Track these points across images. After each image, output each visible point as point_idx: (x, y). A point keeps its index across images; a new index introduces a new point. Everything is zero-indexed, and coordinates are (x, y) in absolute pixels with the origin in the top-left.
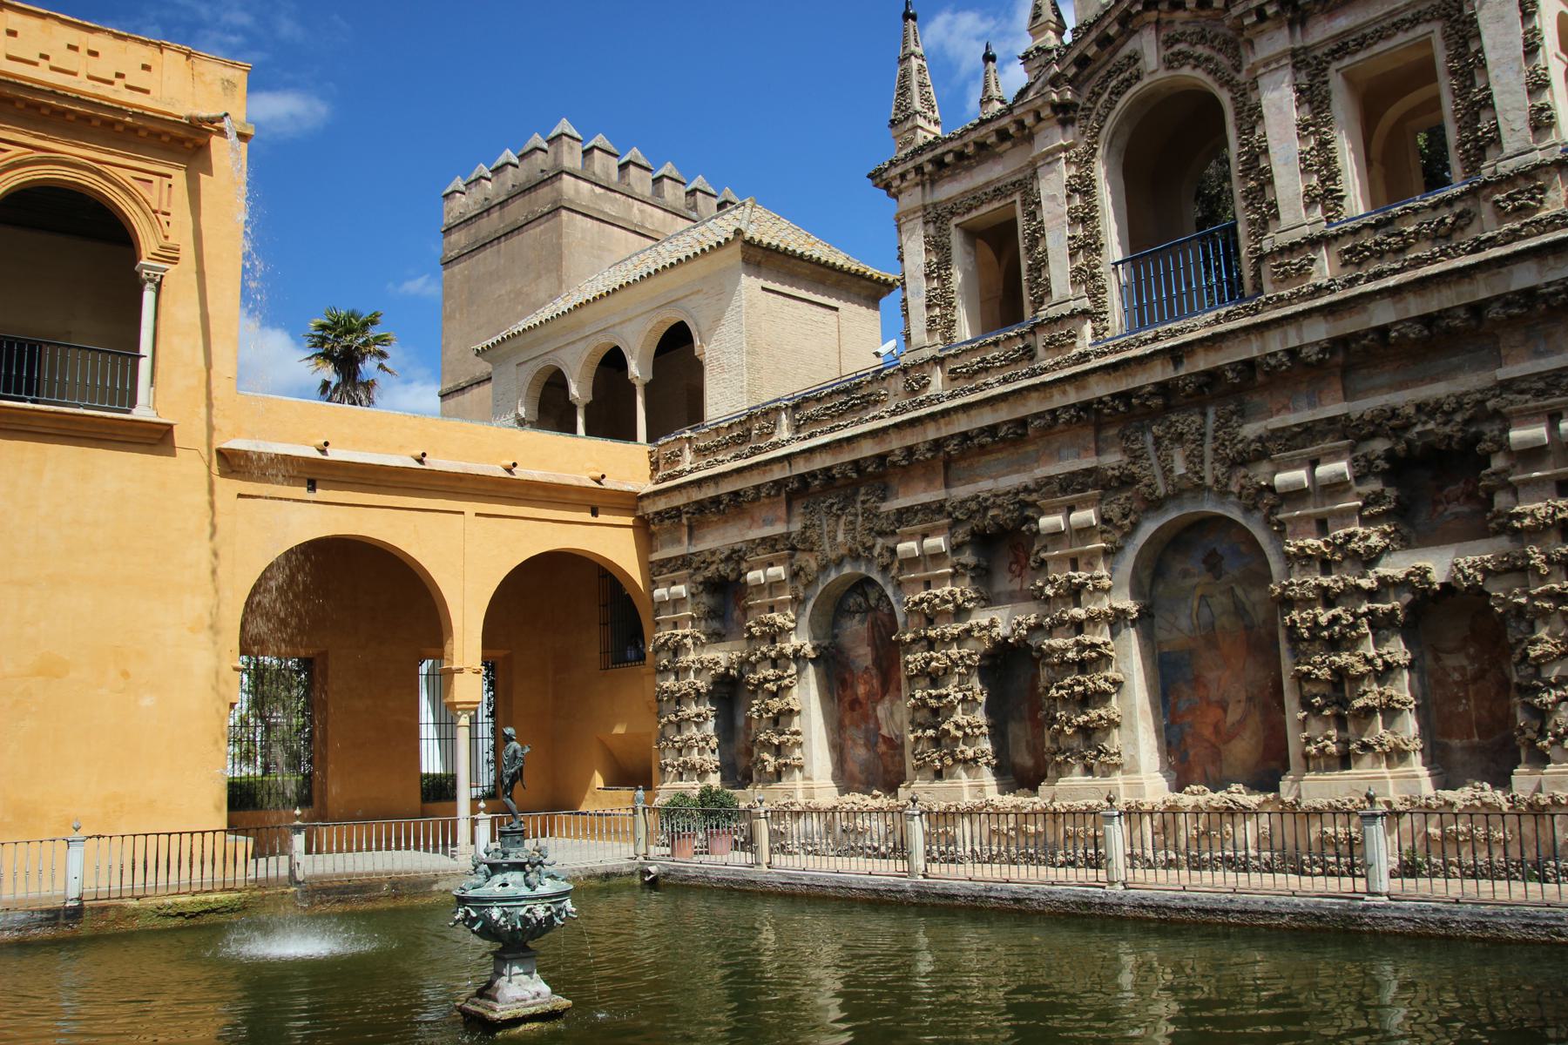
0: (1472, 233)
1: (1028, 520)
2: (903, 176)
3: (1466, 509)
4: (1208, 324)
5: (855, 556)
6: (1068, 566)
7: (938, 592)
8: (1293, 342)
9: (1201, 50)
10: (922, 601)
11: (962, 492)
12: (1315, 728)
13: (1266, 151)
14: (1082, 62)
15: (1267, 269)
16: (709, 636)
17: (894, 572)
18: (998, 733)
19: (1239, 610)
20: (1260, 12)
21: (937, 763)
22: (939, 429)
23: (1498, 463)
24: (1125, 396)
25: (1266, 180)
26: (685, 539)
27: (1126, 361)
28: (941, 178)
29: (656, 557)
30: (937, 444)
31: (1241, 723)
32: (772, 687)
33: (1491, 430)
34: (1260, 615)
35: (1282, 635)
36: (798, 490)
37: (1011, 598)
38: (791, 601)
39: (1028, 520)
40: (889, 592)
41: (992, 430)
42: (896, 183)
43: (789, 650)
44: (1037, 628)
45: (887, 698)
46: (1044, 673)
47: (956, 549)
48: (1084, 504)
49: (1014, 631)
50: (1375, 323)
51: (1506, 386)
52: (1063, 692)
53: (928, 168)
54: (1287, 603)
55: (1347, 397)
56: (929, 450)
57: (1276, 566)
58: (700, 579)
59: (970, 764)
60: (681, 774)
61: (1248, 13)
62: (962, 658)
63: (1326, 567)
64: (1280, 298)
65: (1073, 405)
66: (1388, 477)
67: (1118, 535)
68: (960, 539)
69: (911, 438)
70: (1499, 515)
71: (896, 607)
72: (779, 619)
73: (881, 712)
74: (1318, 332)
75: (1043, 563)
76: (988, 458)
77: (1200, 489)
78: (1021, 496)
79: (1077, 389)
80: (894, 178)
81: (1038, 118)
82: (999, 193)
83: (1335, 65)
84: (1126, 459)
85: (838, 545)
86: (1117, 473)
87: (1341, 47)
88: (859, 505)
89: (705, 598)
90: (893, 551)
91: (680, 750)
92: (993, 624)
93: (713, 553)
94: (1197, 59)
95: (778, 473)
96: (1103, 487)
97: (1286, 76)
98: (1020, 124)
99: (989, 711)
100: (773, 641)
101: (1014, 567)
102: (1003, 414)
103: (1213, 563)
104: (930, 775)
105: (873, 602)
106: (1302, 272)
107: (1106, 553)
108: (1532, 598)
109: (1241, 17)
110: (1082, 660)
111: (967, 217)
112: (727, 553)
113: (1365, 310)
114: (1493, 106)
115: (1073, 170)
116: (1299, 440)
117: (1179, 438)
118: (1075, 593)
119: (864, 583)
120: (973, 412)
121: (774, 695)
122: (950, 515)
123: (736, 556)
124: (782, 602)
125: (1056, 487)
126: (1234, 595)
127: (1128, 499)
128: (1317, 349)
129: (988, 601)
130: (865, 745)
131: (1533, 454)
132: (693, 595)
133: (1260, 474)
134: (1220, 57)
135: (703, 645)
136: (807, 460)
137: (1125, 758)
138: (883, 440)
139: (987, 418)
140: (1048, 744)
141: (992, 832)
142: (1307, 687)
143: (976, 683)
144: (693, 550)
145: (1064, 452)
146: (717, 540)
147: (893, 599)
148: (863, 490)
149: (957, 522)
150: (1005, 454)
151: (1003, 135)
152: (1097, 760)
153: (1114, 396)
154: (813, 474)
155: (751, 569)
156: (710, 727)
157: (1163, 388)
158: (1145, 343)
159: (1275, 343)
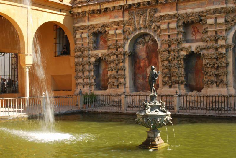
1: (201, 20)
5: (145, 27)
6: (214, 34)
7: (173, 38)
10: (168, 40)
11: (181, 12)
16: (93, 48)
17: (158, 32)
18: (186, 77)
21: (171, 84)
26: (87, 21)
29: (77, 25)
32: (116, 62)
36: (128, 8)
37: (192, 41)
38: (123, 39)
39: (201, 20)
40: (156, 38)
43: (123, 53)
44: (204, 48)
46: (205, 61)
47: (178, 27)
49: (196, 49)
52: (211, 66)
58: (92, 31)
60: (84, 86)
62: (179, 56)
67: (230, 25)
68: (180, 24)
71: (158, 42)
72: (120, 44)
75: (207, 32)
76: (190, 3)
78: (201, 14)
85: (140, 25)
86: (231, 9)
88: (148, 14)
89: (92, 37)
90: (159, 27)
91: (83, 80)
92: (190, 47)
93: (96, 25)
96: (226, 13)
99: (185, 70)
100: (117, 50)
101: (193, 33)
104: (167, 86)
105: (147, 41)
107: (226, 30)
110: (218, 58)
112: (102, 25)
118: (216, 40)
119: (144, 35)
121: (117, 65)
122: (177, 18)
123: (104, 26)
124: (121, 40)
125: (212, 11)
129: (187, 41)
130: (142, 79)
132: (89, 36)
135: (92, 50)
137: (229, 83)
140: (205, 79)
141: (187, 101)
143: (182, 62)
144: (90, 23)
145: (215, 3)
146: (98, 21)
147: (157, 40)
148: (149, 10)
152: (220, 82)
154: (134, 5)
155: (109, 30)
156: (92, 73)
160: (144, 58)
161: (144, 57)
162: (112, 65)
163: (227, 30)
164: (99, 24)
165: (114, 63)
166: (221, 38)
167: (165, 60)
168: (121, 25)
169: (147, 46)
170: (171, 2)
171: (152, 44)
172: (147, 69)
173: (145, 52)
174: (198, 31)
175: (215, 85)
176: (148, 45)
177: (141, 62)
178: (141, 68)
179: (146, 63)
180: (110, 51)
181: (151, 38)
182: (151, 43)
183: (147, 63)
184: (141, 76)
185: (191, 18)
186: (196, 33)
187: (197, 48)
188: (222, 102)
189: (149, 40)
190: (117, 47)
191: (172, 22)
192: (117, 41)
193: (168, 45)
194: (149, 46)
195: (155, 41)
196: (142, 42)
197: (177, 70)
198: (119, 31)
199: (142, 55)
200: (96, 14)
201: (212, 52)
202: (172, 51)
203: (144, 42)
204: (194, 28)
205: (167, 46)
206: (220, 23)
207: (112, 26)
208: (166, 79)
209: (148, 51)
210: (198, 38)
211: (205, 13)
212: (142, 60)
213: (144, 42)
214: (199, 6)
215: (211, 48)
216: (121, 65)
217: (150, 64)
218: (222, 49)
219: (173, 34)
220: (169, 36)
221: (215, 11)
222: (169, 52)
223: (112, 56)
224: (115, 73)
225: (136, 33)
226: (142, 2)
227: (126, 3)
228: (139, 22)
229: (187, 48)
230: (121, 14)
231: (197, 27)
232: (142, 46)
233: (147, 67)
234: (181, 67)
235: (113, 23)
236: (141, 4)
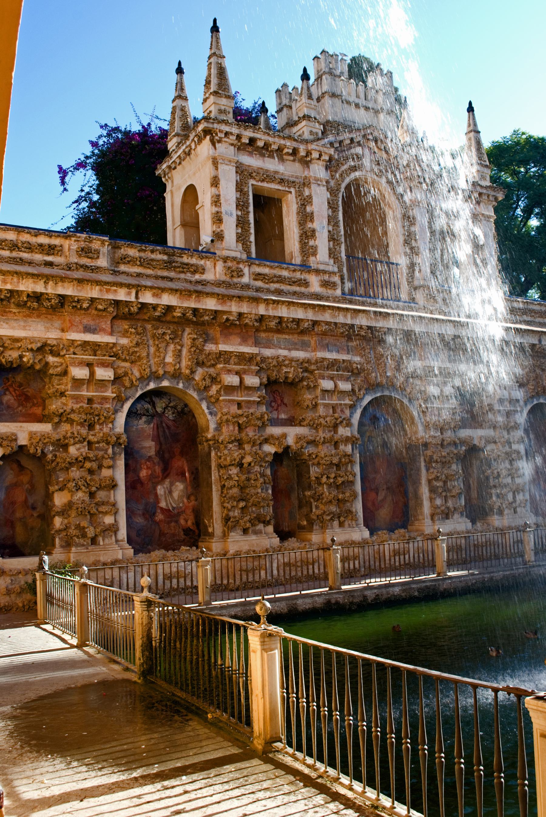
2: (227, 134)
6: (331, 411)
11: (268, 352)
14: (341, 142)
22: (267, 310)
28: (244, 150)
30: (261, 319)
31: (383, 500)
32: (94, 465)
35: (422, 459)
41: (298, 321)
42: (219, 135)
45: (167, 482)
46: (314, 471)
48: (341, 378)
49: (297, 443)
53: (246, 140)
56: (256, 320)
59: (266, 523)
65: (346, 324)
69: (245, 308)
73: (160, 490)
80: (221, 131)
81: (320, 155)
82: (282, 181)
84: (363, 361)
95: (122, 295)
98: (309, 153)
100: (91, 427)
101: (273, 404)
102: (310, 315)
111: (260, 184)
115: (329, 196)
120: (292, 308)
122: (257, 364)
136: (154, 295)
138: (223, 303)
139: (300, 314)
142: (435, 483)
143: (268, 472)
149: (261, 369)
150: (291, 337)
151: (295, 152)
152: (344, 516)
154: (155, 307)
160: (150, 457)
161: (149, 454)
162: (75, 473)
163: (352, 407)
164: (26, 338)
165: (82, 467)
166: (344, 422)
167: (233, 465)
168: (104, 355)
169: (159, 423)
170: (251, 324)
171: (174, 421)
172: (159, 487)
173: (153, 440)
174: (282, 401)
175: (336, 523)
176: (161, 422)
177: (141, 468)
178: (142, 484)
179: (155, 472)
180: (65, 427)
181: (172, 404)
182: (171, 417)
183: (158, 469)
184: (141, 507)
185: (285, 370)
186: (278, 406)
187: (299, 439)
188: (355, 558)
189: (165, 408)
190: (97, 418)
191: (245, 372)
192: (90, 401)
193: (239, 425)
194: (164, 425)
195: (186, 414)
196: (146, 413)
197: (260, 491)
198: (104, 374)
199: (145, 448)
200: (12, 305)
201: (324, 450)
202: (248, 443)
203: (151, 411)
204: (274, 392)
205: (237, 428)
206: (341, 392)
207: (74, 354)
208: (236, 513)
209: (162, 439)
210: (283, 416)
211: (314, 364)
212: (143, 461)
213: (151, 411)
214: (297, 347)
215: (328, 442)
216: (106, 473)
217: (166, 472)
218: (346, 445)
219: (249, 402)
220: (239, 405)
221: (333, 364)
222: (240, 443)
223: (74, 444)
224: (87, 498)
225: (148, 384)
226: (180, 307)
227: (137, 297)
228: (164, 359)
229: (278, 439)
230: (106, 324)
231: (280, 391)
232: (145, 422)
233: (158, 483)
234: (267, 481)
235: (80, 345)
236: (178, 310)
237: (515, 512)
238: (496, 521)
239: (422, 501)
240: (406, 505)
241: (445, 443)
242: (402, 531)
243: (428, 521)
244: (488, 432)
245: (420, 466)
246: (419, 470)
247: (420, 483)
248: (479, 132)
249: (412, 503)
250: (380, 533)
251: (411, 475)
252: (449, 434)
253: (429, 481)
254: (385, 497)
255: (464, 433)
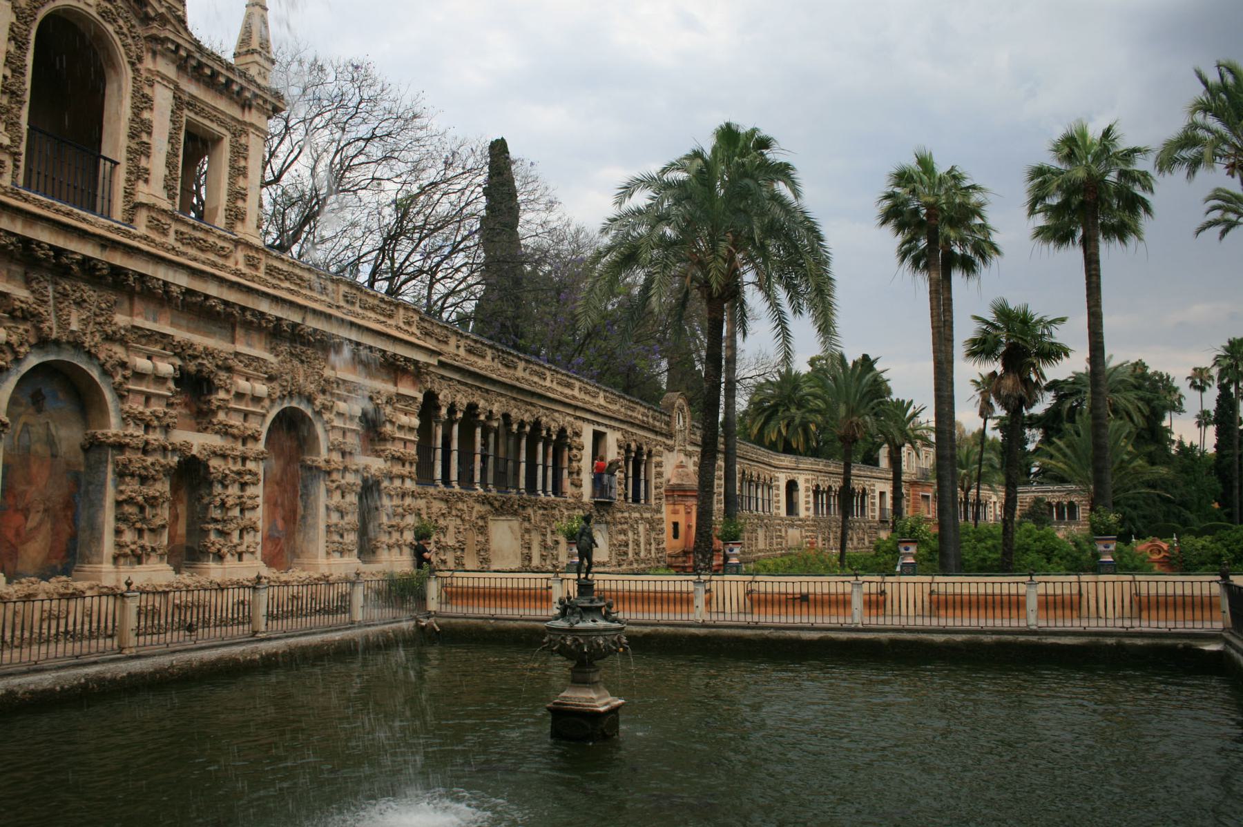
0: (230, 263)
3: (184, 411)
4: (103, 227)
8: (170, 279)
9: (121, 22)
12: (128, 537)
13: (150, 134)
15: (142, 217)
19: (51, 442)
20: (178, 46)
23: (222, 395)
24: (59, 252)
25: (144, 150)
27: (76, 229)
33: (223, 375)
34: (63, 448)
35: (110, 468)
50: (208, 292)
51: (237, 354)
54: (121, 447)
55: (172, 324)
57: (114, 420)
61: (173, 42)
63: (148, 427)
64: (153, 241)
66: (177, 382)
70: (220, 423)
74: (182, 280)
77: (77, 345)
79: (24, 227)
83: (186, 112)
84: (31, 299)
87: (193, 103)
94: (121, 28)
97: (169, 94)
103: (37, 401)
106: (164, 233)
108: (233, 472)
109: (167, 39)
113: (206, 281)
114: (245, 201)
116: (144, 341)
117: (80, 304)
126: (48, 429)
127: (27, 331)
128: (178, 290)
131: (240, 396)
133: (119, 352)
134: (130, 41)
142: (128, 509)
153: (52, 247)
157: (87, 263)
158: (58, 211)
159: (162, 273)
237: (240, 559)
238: (214, 571)
239: (102, 534)
240: (74, 537)
241: (150, 447)
242: (64, 578)
243: (107, 566)
244: (215, 441)
245: (105, 479)
246: (103, 485)
247: (102, 506)
248: (266, 9)
249: (83, 536)
250: (23, 580)
251: (87, 492)
252: (156, 437)
253: (119, 504)
254: (40, 524)
255: (180, 436)
